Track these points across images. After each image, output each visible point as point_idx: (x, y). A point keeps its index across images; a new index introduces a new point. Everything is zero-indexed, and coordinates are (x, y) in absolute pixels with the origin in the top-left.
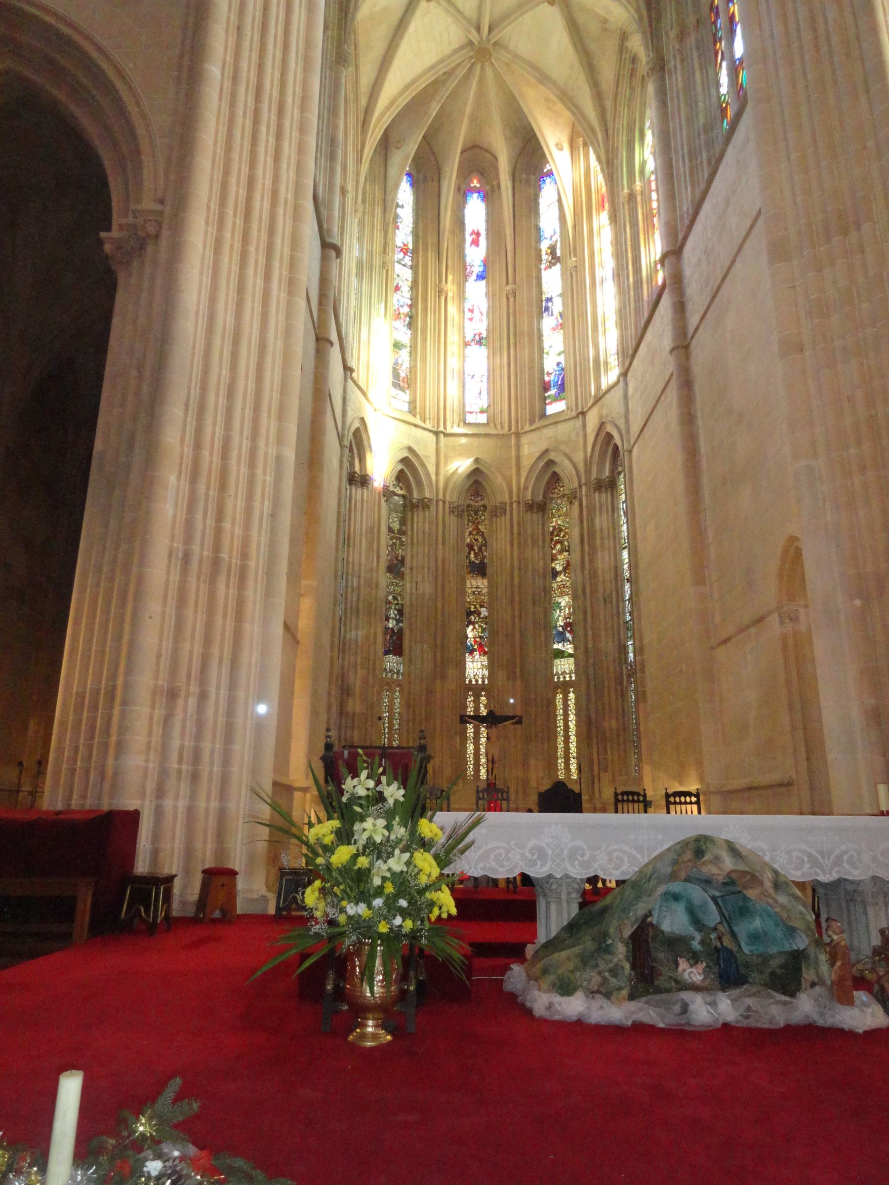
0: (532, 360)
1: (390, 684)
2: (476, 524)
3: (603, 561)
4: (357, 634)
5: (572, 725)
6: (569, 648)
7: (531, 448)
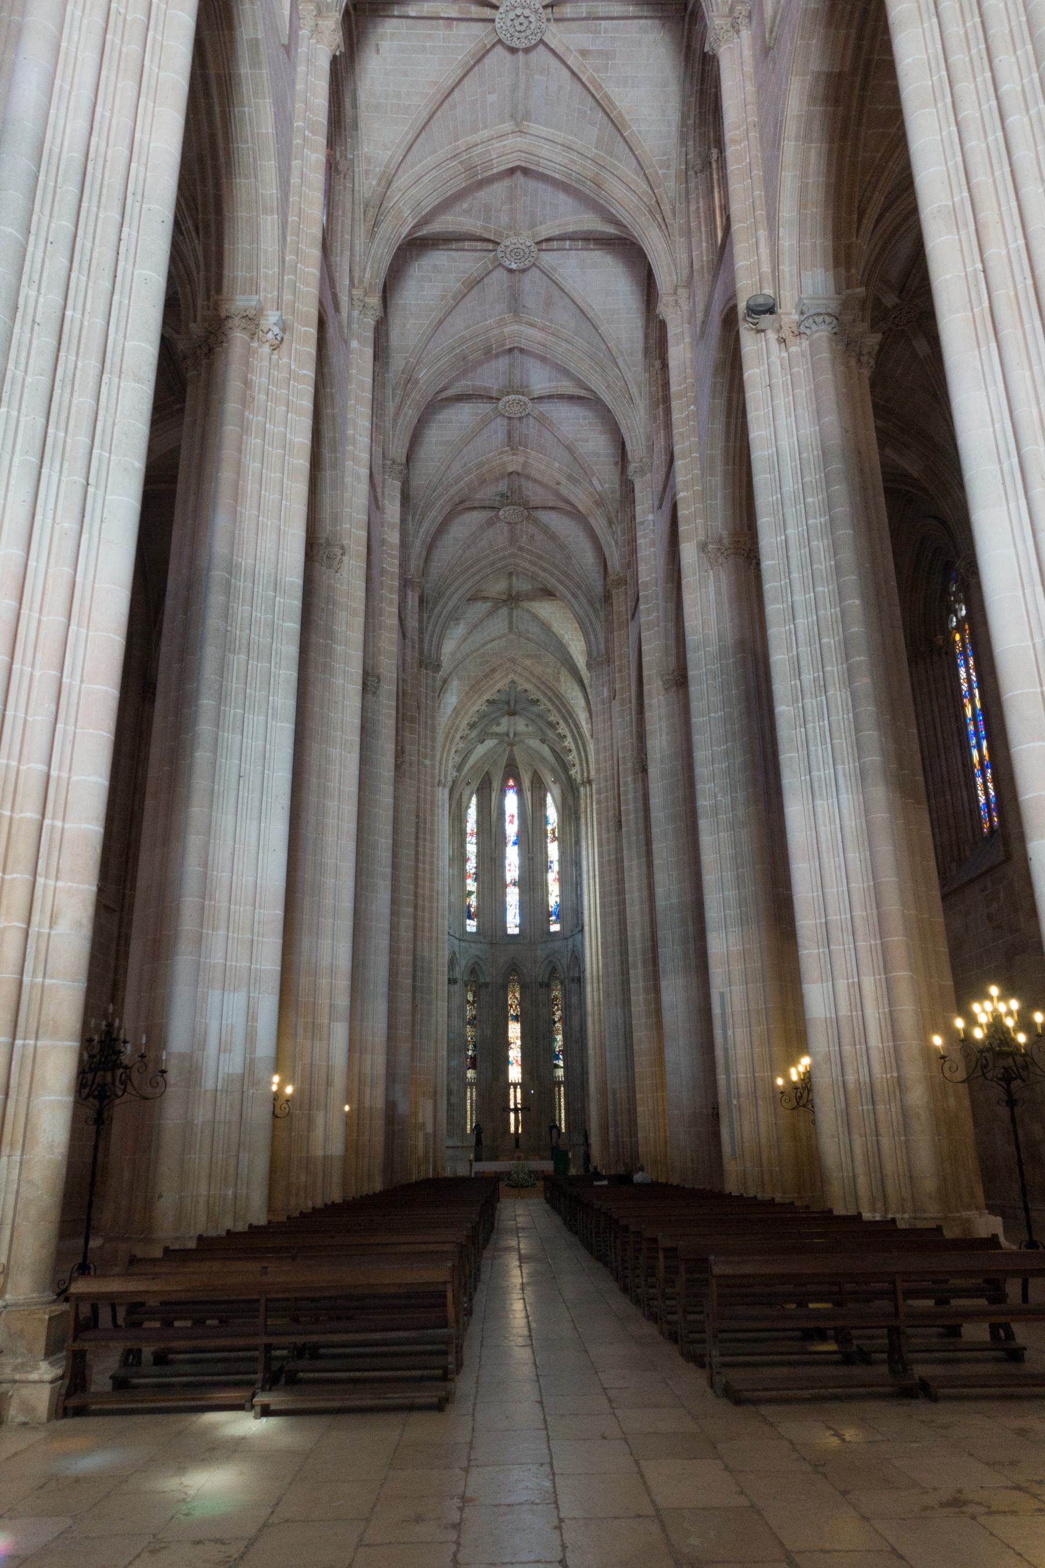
0: (543, 899)
1: (471, 1085)
2: (514, 993)
3: (575, 1021)
4: (454, 1063)
5: (562, 1104)
6: (561, 1063)
7: (540, 952)
